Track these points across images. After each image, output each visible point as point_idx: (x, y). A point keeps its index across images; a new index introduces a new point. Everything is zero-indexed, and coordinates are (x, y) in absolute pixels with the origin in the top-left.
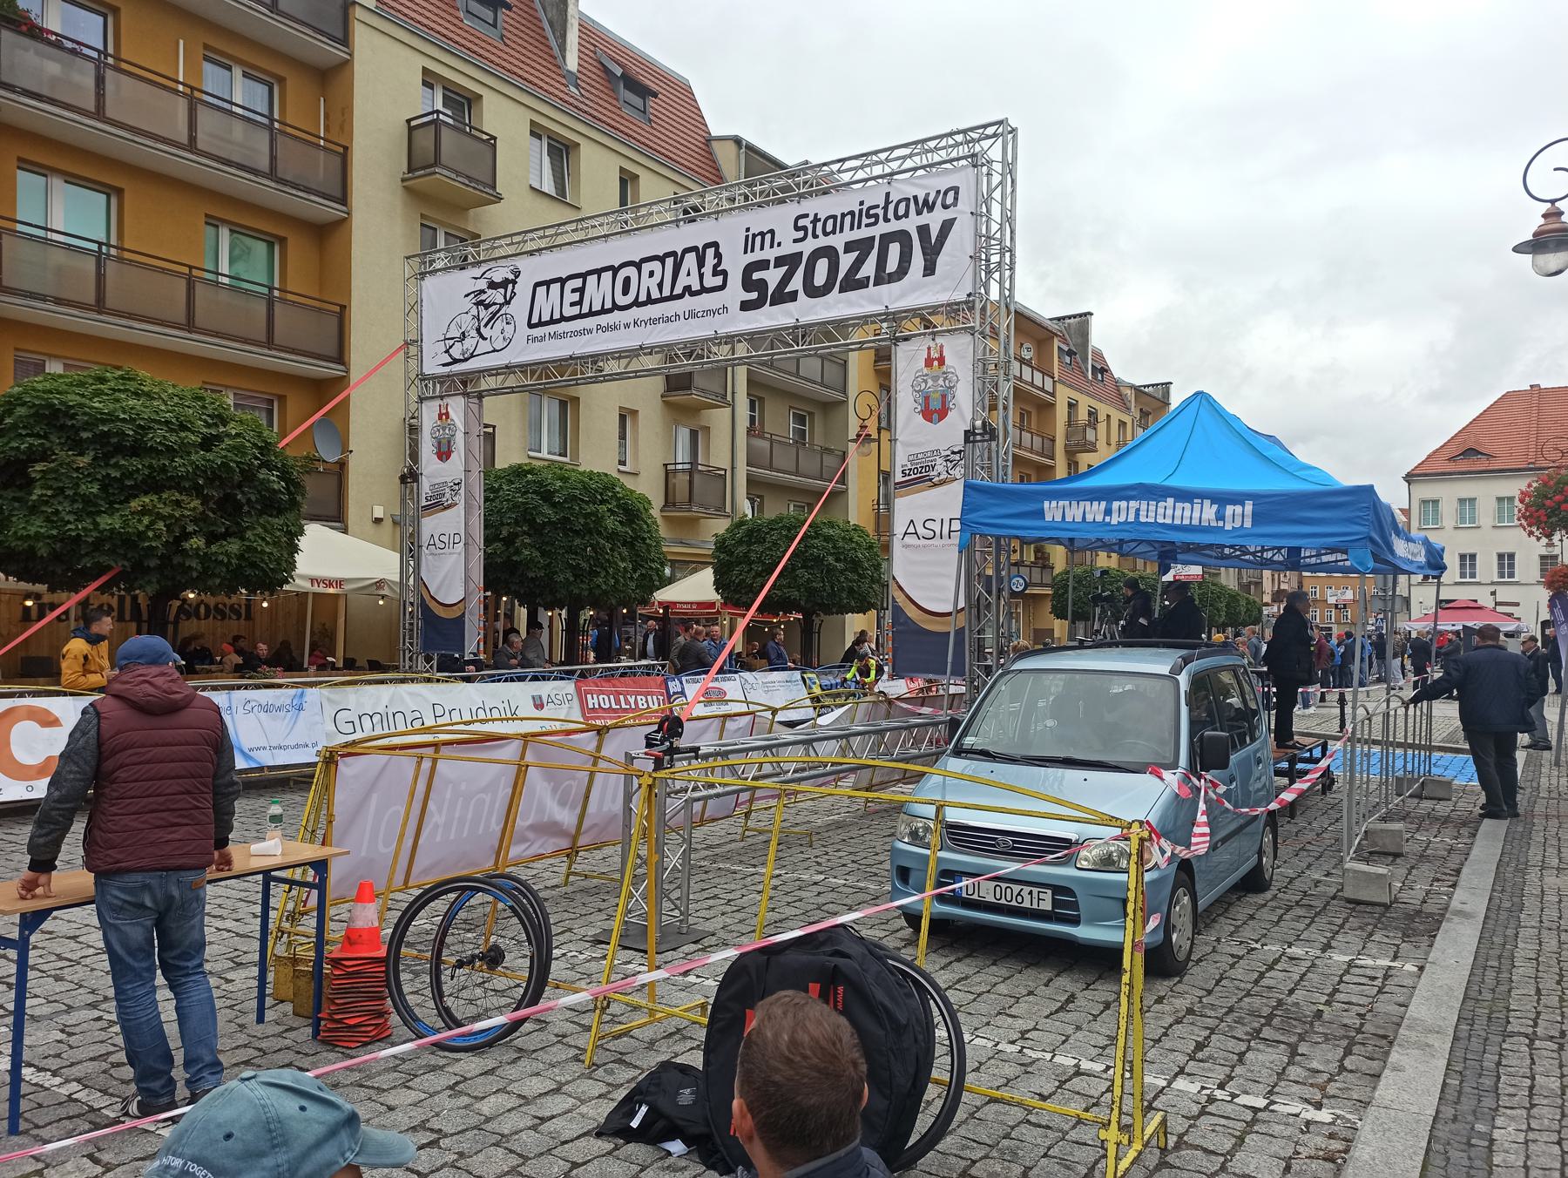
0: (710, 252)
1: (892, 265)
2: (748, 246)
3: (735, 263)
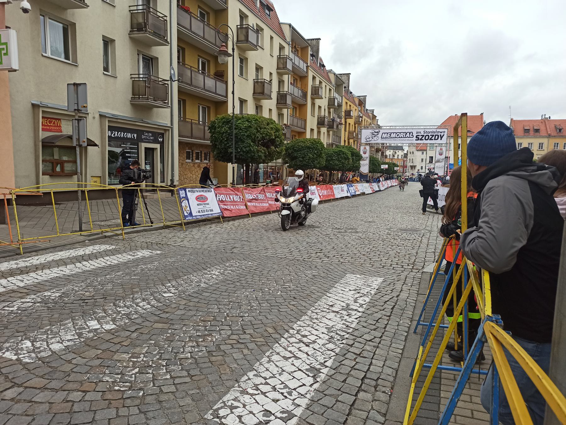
1: (436, 138)
2: (417, 133)
3: (415, 135)
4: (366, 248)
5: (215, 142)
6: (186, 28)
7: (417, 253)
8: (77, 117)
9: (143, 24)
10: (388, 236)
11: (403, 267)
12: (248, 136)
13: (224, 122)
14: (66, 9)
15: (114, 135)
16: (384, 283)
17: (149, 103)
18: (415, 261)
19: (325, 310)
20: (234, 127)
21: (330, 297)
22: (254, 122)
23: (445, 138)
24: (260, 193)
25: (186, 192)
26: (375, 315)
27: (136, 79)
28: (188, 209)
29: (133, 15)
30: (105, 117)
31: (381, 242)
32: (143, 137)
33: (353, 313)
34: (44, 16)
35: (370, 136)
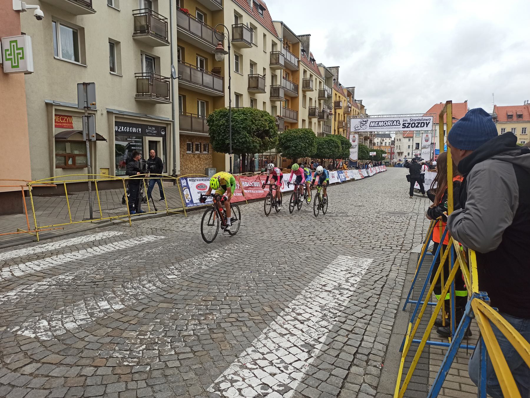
0: (398, 121)
1: (422, 125)
2: (404, 121)
3: (402, 123)
4: (356, 231)
5: (213, 134)
6: (185, 29)
7: (405, 235)
8: (86, 114)
9: (146, 26)
10: (377, 219)
11: (391, 248)
12: (243, 128)
13: (221, 115)
14: (76, 15)
15: (121, 130)
16: (374, 264)
17: (152, 99)
18: (403, 243)
19: (318, 289)
20: (231, 120)
21: (322, 277)
22: (249, 114)
23: (430, 125)
24: (255, 181)
25: (187, 181)
26: (366, 293)
27: (140, 78)
28: (189, 197)
29: (136, 18)
30: (112, 113)
31: (371, 225)
32: (147, 131)
33: (345, 292)
34: (55, 22)
35: (359, 125)
